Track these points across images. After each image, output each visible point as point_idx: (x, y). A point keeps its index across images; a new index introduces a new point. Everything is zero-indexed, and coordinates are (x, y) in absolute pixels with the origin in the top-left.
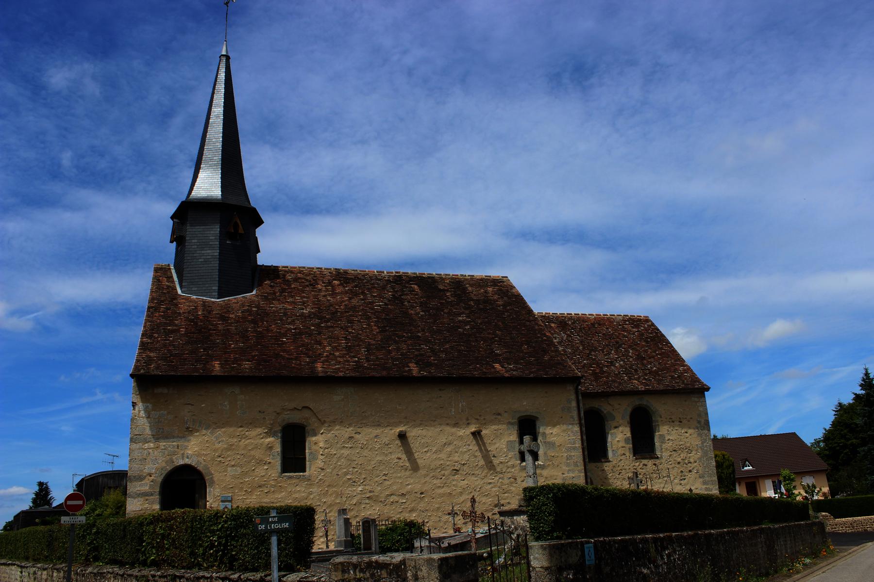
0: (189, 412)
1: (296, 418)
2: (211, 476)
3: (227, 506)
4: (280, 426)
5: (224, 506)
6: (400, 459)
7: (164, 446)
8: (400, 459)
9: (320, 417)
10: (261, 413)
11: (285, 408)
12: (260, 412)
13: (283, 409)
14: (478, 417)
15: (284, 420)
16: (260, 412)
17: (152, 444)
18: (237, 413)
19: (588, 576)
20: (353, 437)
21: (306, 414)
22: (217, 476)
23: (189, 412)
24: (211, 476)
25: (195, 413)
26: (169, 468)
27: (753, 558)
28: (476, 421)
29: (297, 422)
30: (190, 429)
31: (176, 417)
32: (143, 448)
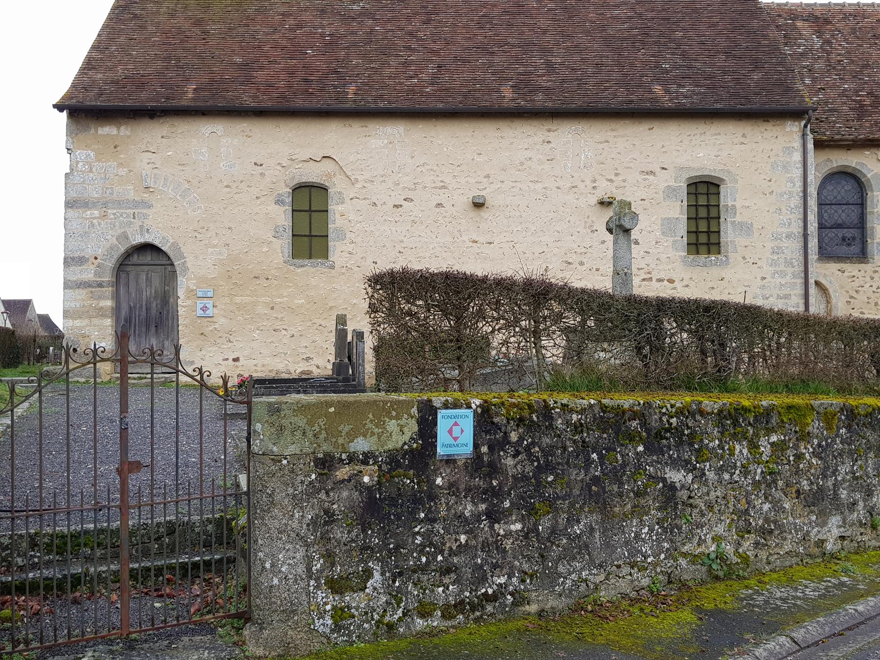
0: (148, 164)
1: (312, 174)
2: (183, 261)
3: (207, 305)
4: (287, 186)
5: (203, 305)
6: (476, 242)
7: (114, 214)
8: (476, 242)
9: (349, 173)
10: (258, 165)
11: (293, 157)
12: (255, 164)
13: (292, 160)
14: (613, 177)
15: (293, 178)
16: (255, 164)
17: (96, 212)
18: (221, 165)
19: (439, 481)
20: (401, 206)
21: (328, 166)
22: (190, 262)
23: (148, 164)
24: (183, 261)
25: (156, 166)
26: (122, 250)
27: (794, 481)
28: (609, 183)
29: (314, 181)
30: (151, 190)
31: (130, 171)
32: (83, 218)
